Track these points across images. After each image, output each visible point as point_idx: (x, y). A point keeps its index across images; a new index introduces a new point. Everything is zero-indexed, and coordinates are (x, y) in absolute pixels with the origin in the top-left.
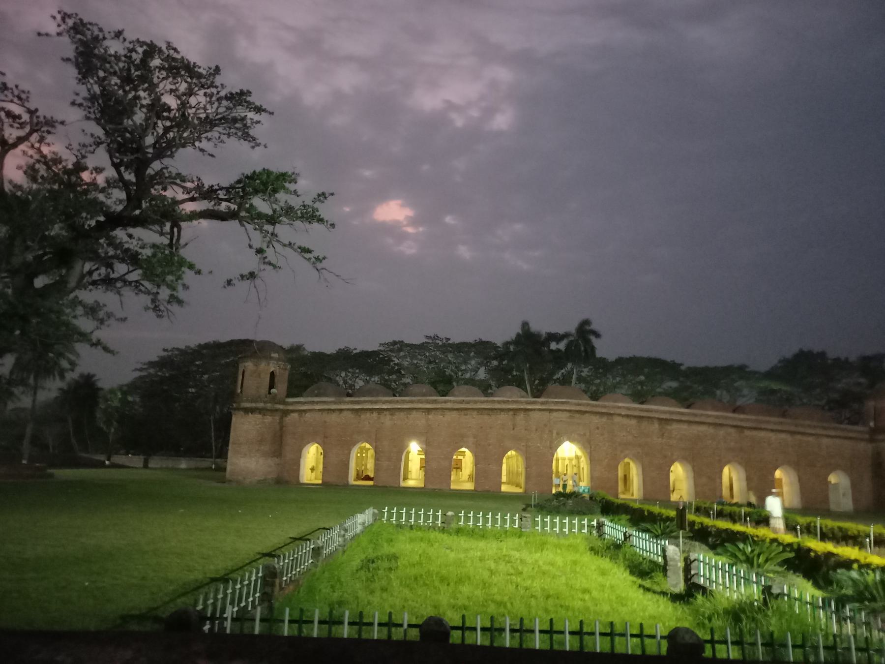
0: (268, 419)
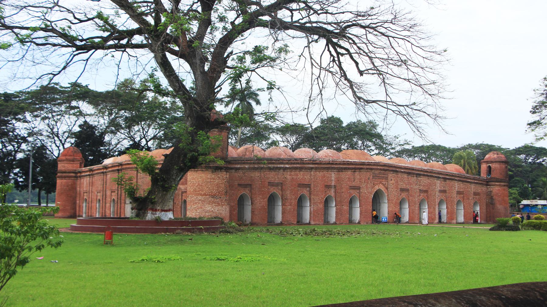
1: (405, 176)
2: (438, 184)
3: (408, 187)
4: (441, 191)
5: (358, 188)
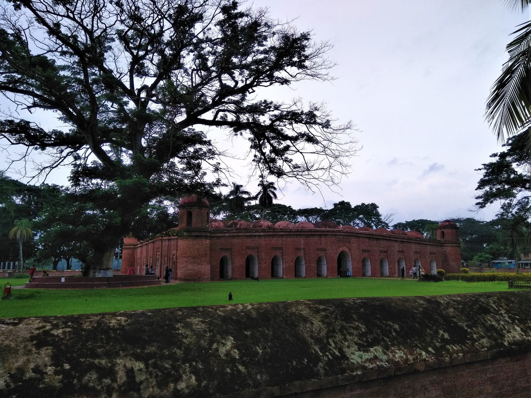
1: (366, 240)
2: (396, 247)
3: (369, 248)
4: (399, 252)
5: (325, 250)
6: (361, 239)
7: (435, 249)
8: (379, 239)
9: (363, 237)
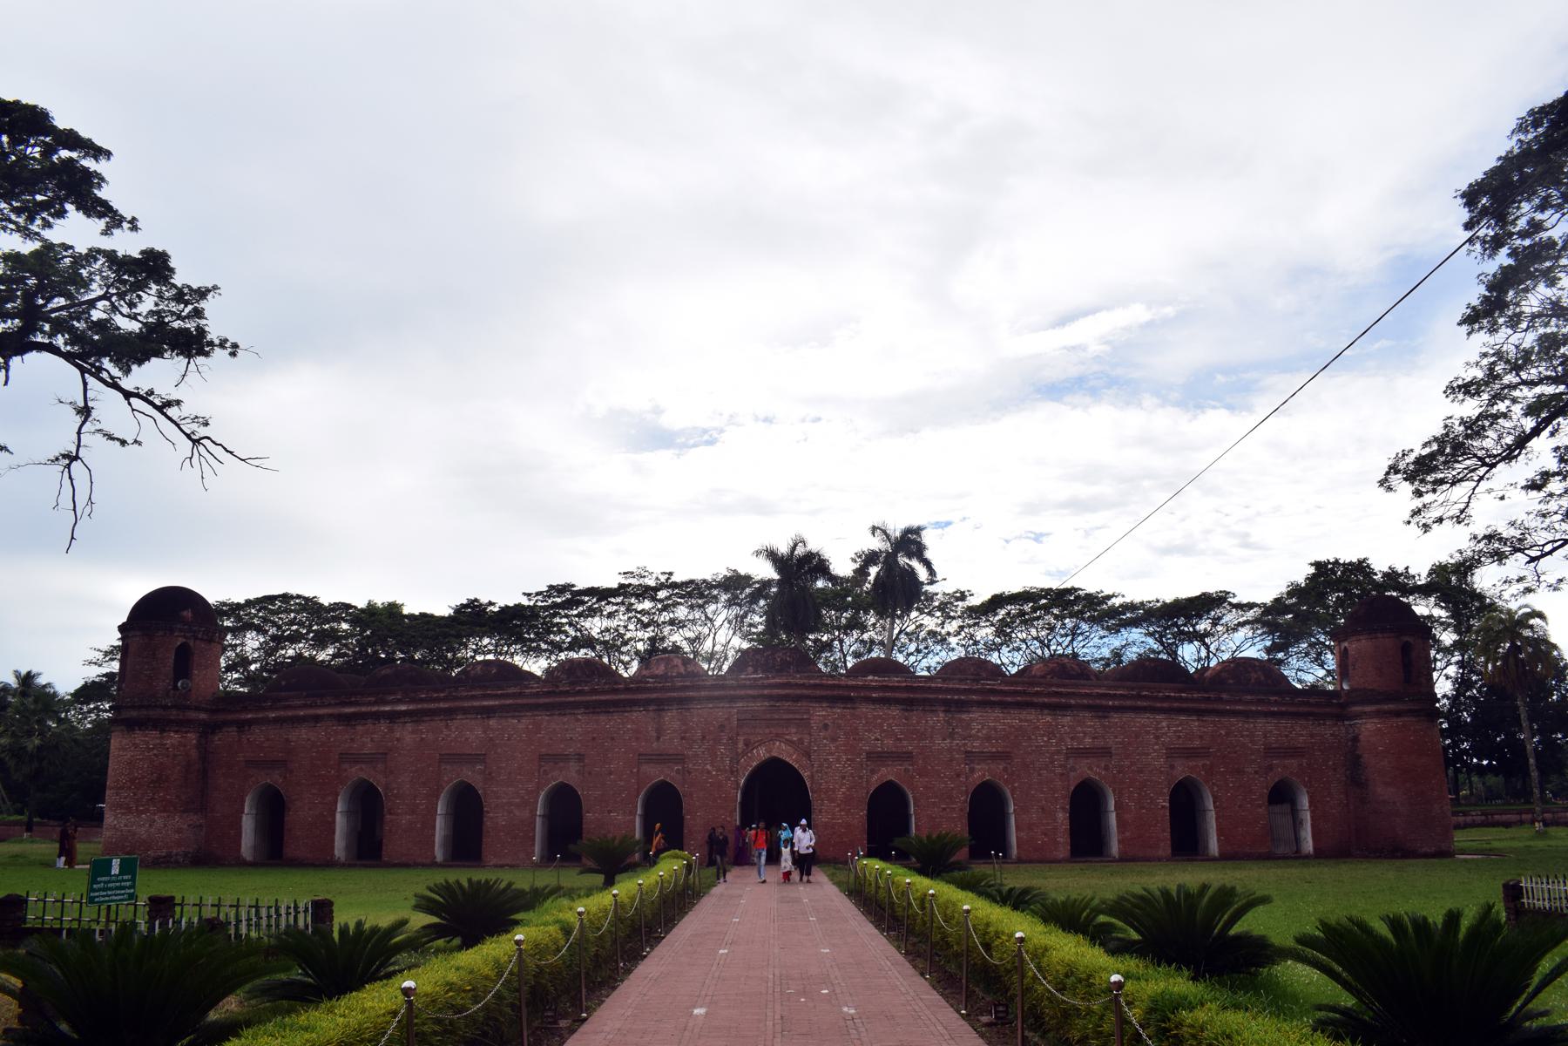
0: (173, 738)
1: (895, 711)
6: (864, 709)
7: (1301, 733)
8: (962, 706)
9: (874, 701)
